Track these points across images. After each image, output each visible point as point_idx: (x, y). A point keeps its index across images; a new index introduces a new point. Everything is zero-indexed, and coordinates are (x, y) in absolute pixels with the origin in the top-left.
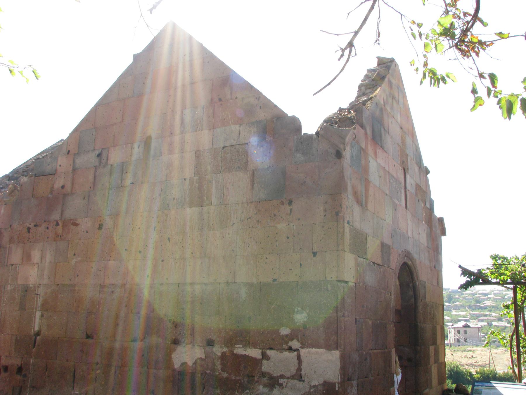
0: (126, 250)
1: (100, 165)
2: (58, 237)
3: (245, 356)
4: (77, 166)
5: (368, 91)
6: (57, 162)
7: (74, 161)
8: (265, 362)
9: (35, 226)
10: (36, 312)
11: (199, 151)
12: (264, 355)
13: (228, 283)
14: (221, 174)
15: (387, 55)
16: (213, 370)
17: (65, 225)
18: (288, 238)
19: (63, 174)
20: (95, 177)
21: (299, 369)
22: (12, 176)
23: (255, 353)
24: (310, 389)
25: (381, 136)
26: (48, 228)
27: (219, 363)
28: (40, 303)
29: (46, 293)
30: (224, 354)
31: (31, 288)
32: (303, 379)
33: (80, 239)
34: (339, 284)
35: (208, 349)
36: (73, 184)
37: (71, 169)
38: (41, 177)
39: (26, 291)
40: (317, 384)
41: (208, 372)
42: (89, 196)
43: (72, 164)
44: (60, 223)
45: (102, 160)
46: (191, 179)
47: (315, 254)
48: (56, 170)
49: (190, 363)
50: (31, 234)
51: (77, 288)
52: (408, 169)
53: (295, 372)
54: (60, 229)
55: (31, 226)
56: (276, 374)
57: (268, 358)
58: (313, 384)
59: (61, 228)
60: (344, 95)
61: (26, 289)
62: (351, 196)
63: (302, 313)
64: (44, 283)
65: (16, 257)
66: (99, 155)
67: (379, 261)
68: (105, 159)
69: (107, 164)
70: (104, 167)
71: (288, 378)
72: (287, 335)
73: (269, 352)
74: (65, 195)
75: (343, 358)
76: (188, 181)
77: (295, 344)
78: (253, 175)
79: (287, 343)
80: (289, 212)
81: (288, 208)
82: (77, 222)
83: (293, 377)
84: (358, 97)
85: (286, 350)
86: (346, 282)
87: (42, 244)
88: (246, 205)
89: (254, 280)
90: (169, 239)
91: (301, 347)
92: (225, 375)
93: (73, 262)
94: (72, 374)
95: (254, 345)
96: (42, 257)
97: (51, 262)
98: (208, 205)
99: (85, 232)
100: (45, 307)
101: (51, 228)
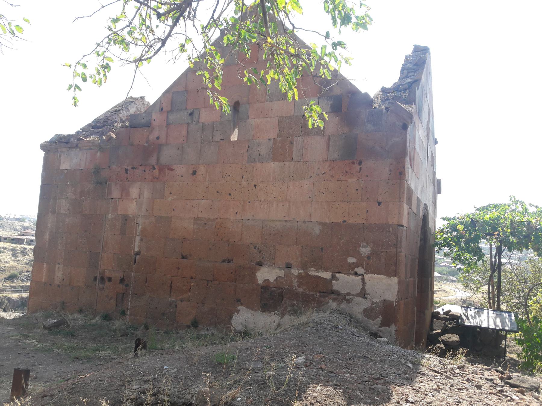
0: (217, 192)
1: (192, 122)
2: (154, 179)
4: (170, 122)
5: (411, 74)
7: (167, 117)
8: (334, 282)
9: (133, 168)
11: (282, 117)
13: (305, 222)
14: (300, 137)
15: (422, 44)
17: (161, 170)
18: (357, 190)
20: (188, 132)
21: (363, 289)
22: (96, 125)
23: (326, 275)
24: (372, 304)
26: (145, 171)
27: (296, 281)
28: (139, 230)
29: (144, 223)
30: (300, 274)
32: (366, 296)
33: (175, 182)
35: (286, 270)
39: (126, 220)
40: (378, 301)
41: (286, 287)
42: (183, 147)
44: (156, 167)
45: (194, 119)
46: (275, 140)
47: (379, 203)
48: (151, 124)
53: (359, 291)
54: (156, 172)
55: (128, 168)
56: (343, 292)
57: (337, 279)
58: (374, 300)
60: (391, 77)
61: (126, 218)
63: (367, 247)
65: (116, 193)
66: (191, 114)
68: (197, 117)
69: (198, 122)
70: (196, 124)
71: (354, 295)
72: (354, 263)
73: (338, 275)
75: (399, 283)
76: (272, 141)
77: (360, 270)
78: (329, 139)
79: (353, 269)
80: (359, 170)
81: (357, 167)
83: (358, 295)
84: (401, 78)
85: (352, 274)
87: (140, 183)
88: (322, 162)
89: (327, 220)
90: (255, 186)
91: (365, 273)
92: (301, 290)
93: (170, 199)
94: (169, 286)
95: (326, 269)
96: (140, 195)
98: (288, 161)
99: (180, 176)
101: (147, 171)
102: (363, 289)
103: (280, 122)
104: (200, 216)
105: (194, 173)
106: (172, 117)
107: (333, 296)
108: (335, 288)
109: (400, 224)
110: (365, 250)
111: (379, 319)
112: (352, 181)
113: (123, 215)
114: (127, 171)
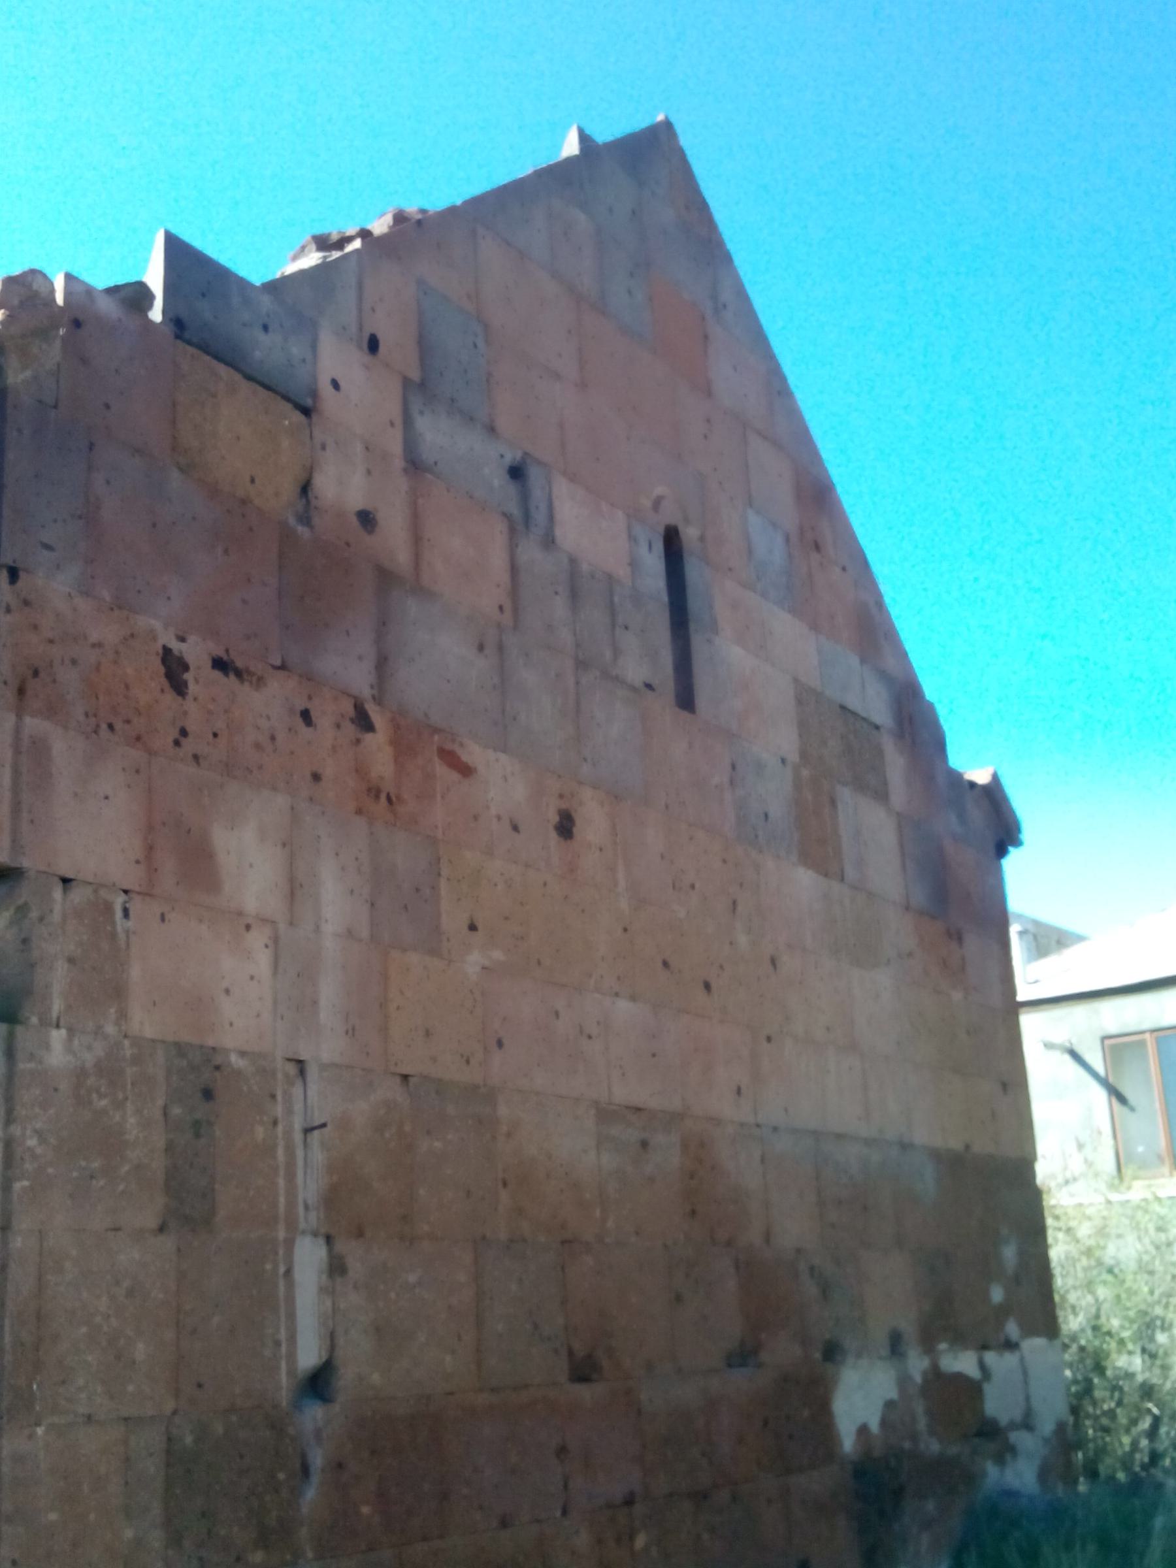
4: (428, 454)
6: (314, 347)
9: (220, 664)
10: (290, 1244)
12: (982, 1366)
16: (914, 1437)
19: (359, 448)
21: (1028, 1399)
26: (306, 716)
28: (310, 1186)
31: (239, 1073)
36: (417, 539)
37: (395, 444)
38: (223, 370)
42: (501, 648)
43: (399, 421)
48: (314, 394)
49: (874, 1426)
50: (189, 705)
51: (503, 1111)
56: (1004, 1420)
59: (388, 751)
61: (203, 1083)
64: (326, 1056)
66: (516, 473)
68: (543, 507)
74: (385, 577)
77: (1012, 1329)
82: (465, 758)
87: (281, 801)
93: (473, 962)
97: (350, 934)
100: (347, 1217)
101: (324, 722)
103: (800, 702)
105: (566, 827)
106: (437, 433)
113: (180, 1049)
114: (174, 670)
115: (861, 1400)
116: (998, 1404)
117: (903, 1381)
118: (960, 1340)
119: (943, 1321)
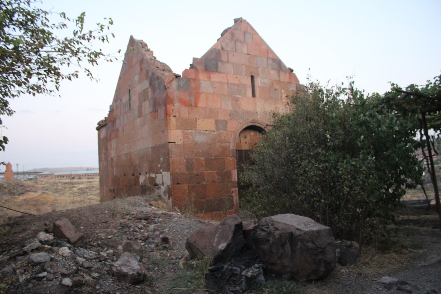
3: (152, 177)
21: (163, 181)
23: (153, 175)
25: (216, 66)
34: (169, 144)
52: (258, 75)
56: (158, 184)
61: (112, 159)
62: (177, 104)
66: (121, 100)
67: (214, 129)
73: (157, 175)
75: (171, 175)
86: (174, 143)
89: (152, 146)
102: (163, 181)
104: (126, 153)
107: (157, 187)
108: (157, 182)
109: (170, 141)
110: (162, 159)
111: (167, 196)
112: (156, 122)
115: (142, 179)
116: (158, 181)
117: (146, 178)
118: (153, 172)
119: (151, 170)
